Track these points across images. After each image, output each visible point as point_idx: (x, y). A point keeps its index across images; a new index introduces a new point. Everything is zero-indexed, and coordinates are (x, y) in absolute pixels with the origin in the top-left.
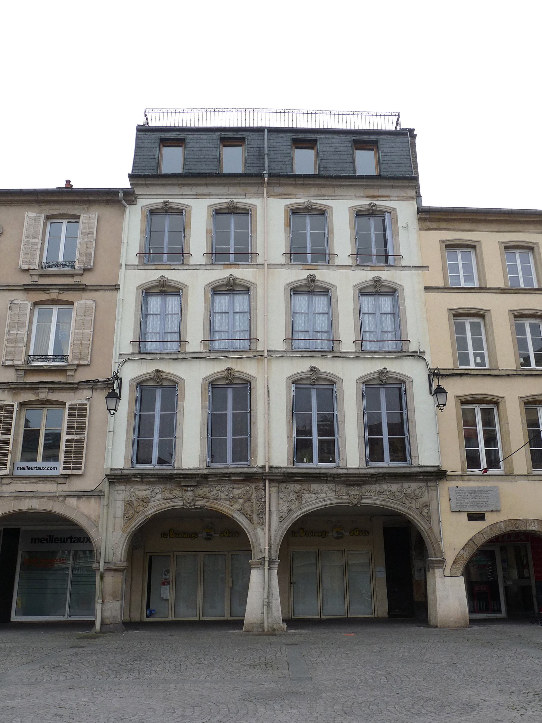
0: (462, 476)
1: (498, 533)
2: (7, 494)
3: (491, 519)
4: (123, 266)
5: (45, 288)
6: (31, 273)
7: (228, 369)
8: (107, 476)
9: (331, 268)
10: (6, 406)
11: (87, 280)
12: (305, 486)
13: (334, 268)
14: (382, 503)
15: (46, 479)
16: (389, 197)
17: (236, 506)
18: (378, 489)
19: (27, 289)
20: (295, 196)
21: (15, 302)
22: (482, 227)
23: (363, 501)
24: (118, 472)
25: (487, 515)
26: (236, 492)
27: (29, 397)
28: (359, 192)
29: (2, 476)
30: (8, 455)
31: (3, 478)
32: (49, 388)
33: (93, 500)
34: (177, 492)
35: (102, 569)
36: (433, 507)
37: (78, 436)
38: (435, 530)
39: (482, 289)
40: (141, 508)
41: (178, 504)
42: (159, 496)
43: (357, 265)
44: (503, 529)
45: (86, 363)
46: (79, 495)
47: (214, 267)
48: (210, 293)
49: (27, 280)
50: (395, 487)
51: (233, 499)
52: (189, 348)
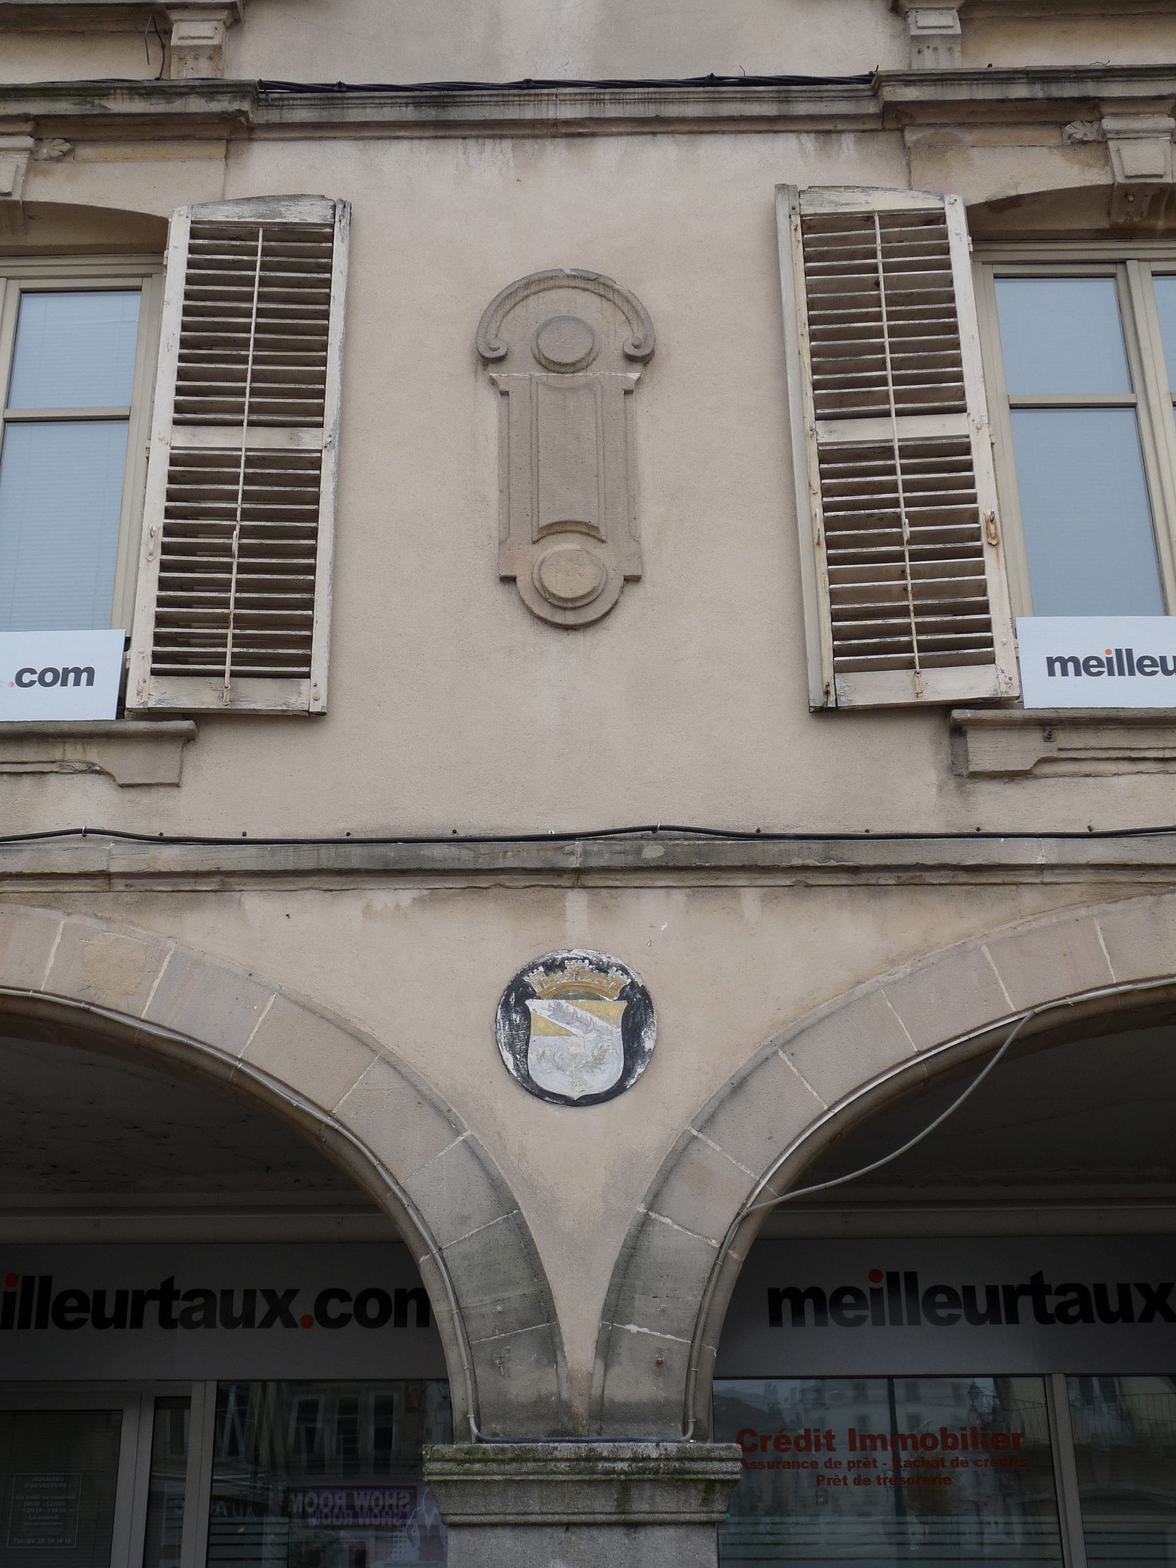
2: (1040, 854)
10: (891, 218)
29: (968, 714)
30: (979, 552)
31: (979, 724)
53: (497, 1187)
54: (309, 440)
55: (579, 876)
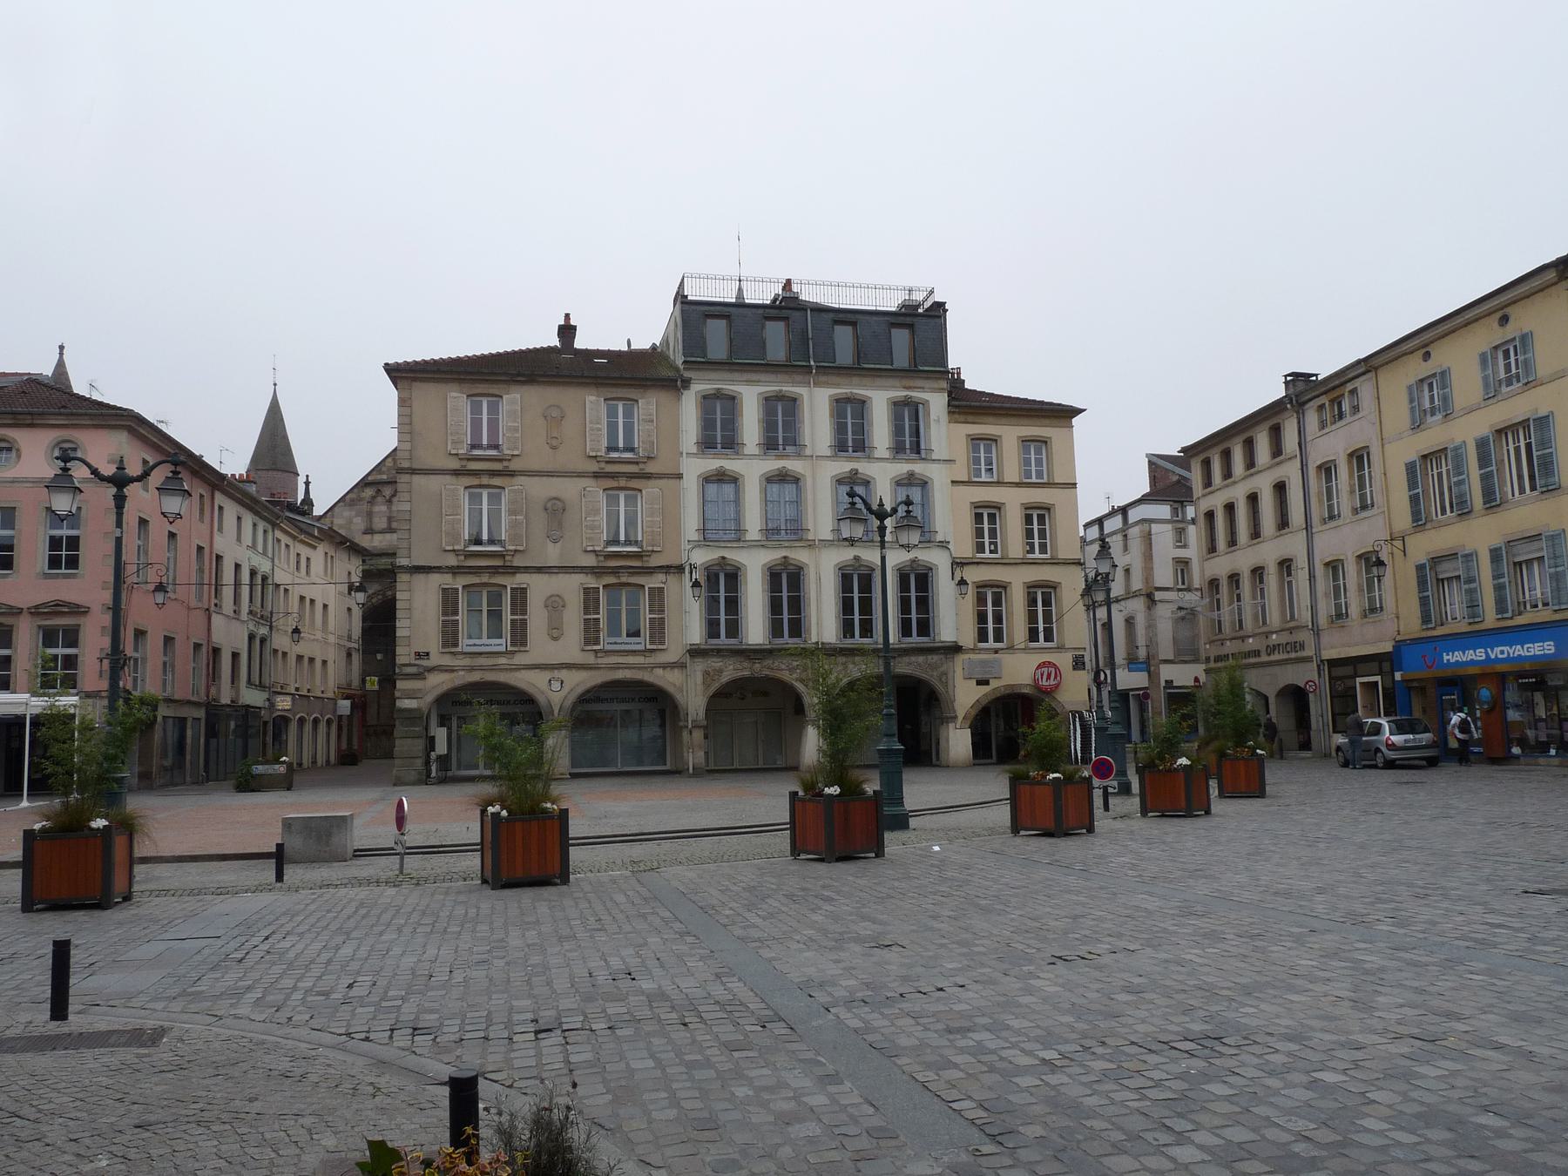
0: (973, 650)
1: (999, 695)
3: (994, 684)
4: (684, 455)
5: (613, 476)
6: (598, 459)
7: (785, 557)
8: (688, 651)
9: (871, 460)
11: (651, 468)
12: (850, 659)
13: (875, 460)
14: (910, 672)
15: (634, 652)
16: (923, 388)
17: (795, 676)
18: (907, 661)
19: (597, 476)
20: (837, 385)
21: (588, 489)
22: (1004, 420)
23: (896, 670)
24: (697, 647)
25: (991, 681)
26: (795, 663)
27: (611, 580)
28: (896, 382)
32: (630, 573)
33: (676, 670)
34: (746, 664)
35: (690, 726)
36: (950, 676)
37: (660, 616)
38: (951, 693)
39: (999, 483)
40: (717, 677)
41: (746, 673)
42: (731, 667)
43: (894, 458)
44: (1003, 691)
45: (659, 549)
46: (664, 666)
47: (767, 457)
48: (765, 483)
49: (594, 467)
50: (921, 659)
51: (792, 670)
52: (749, 537)
53: (549, 701)
54: (526, 617)
55: (556, 669)
